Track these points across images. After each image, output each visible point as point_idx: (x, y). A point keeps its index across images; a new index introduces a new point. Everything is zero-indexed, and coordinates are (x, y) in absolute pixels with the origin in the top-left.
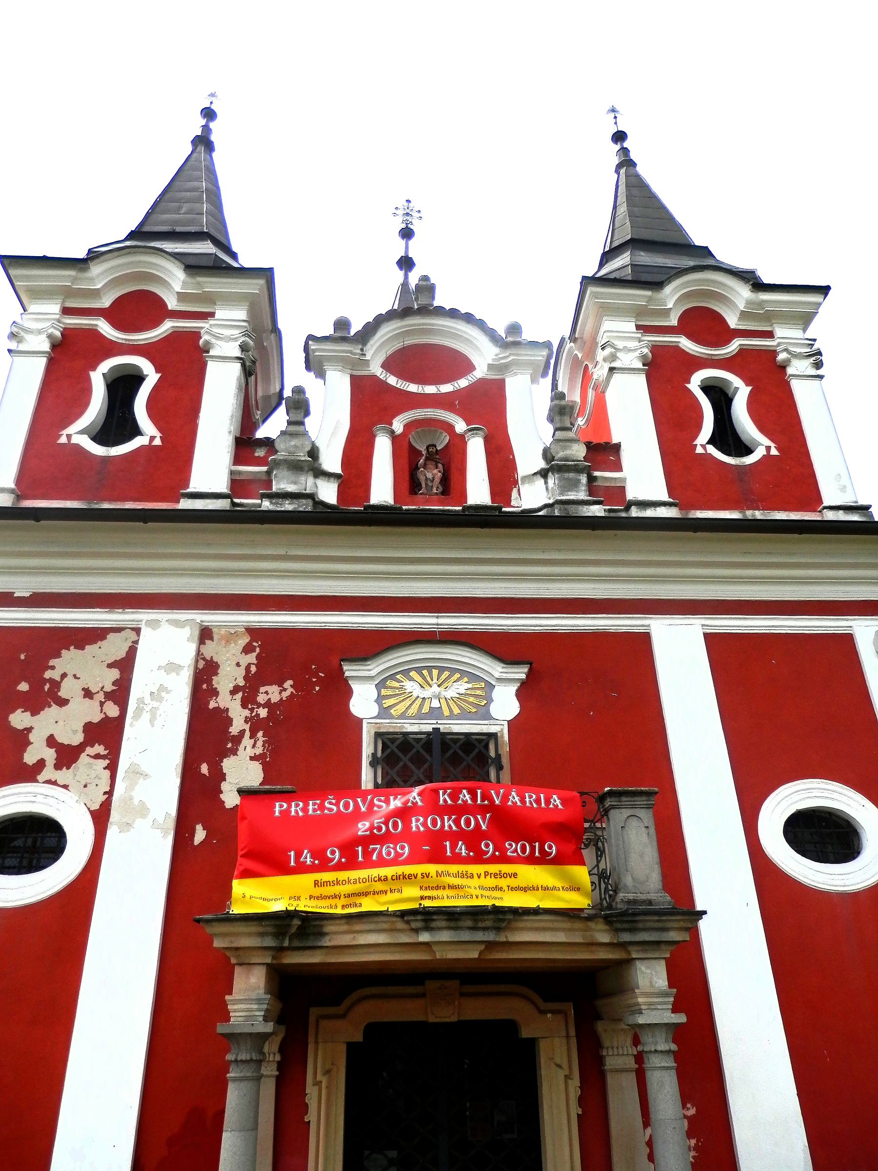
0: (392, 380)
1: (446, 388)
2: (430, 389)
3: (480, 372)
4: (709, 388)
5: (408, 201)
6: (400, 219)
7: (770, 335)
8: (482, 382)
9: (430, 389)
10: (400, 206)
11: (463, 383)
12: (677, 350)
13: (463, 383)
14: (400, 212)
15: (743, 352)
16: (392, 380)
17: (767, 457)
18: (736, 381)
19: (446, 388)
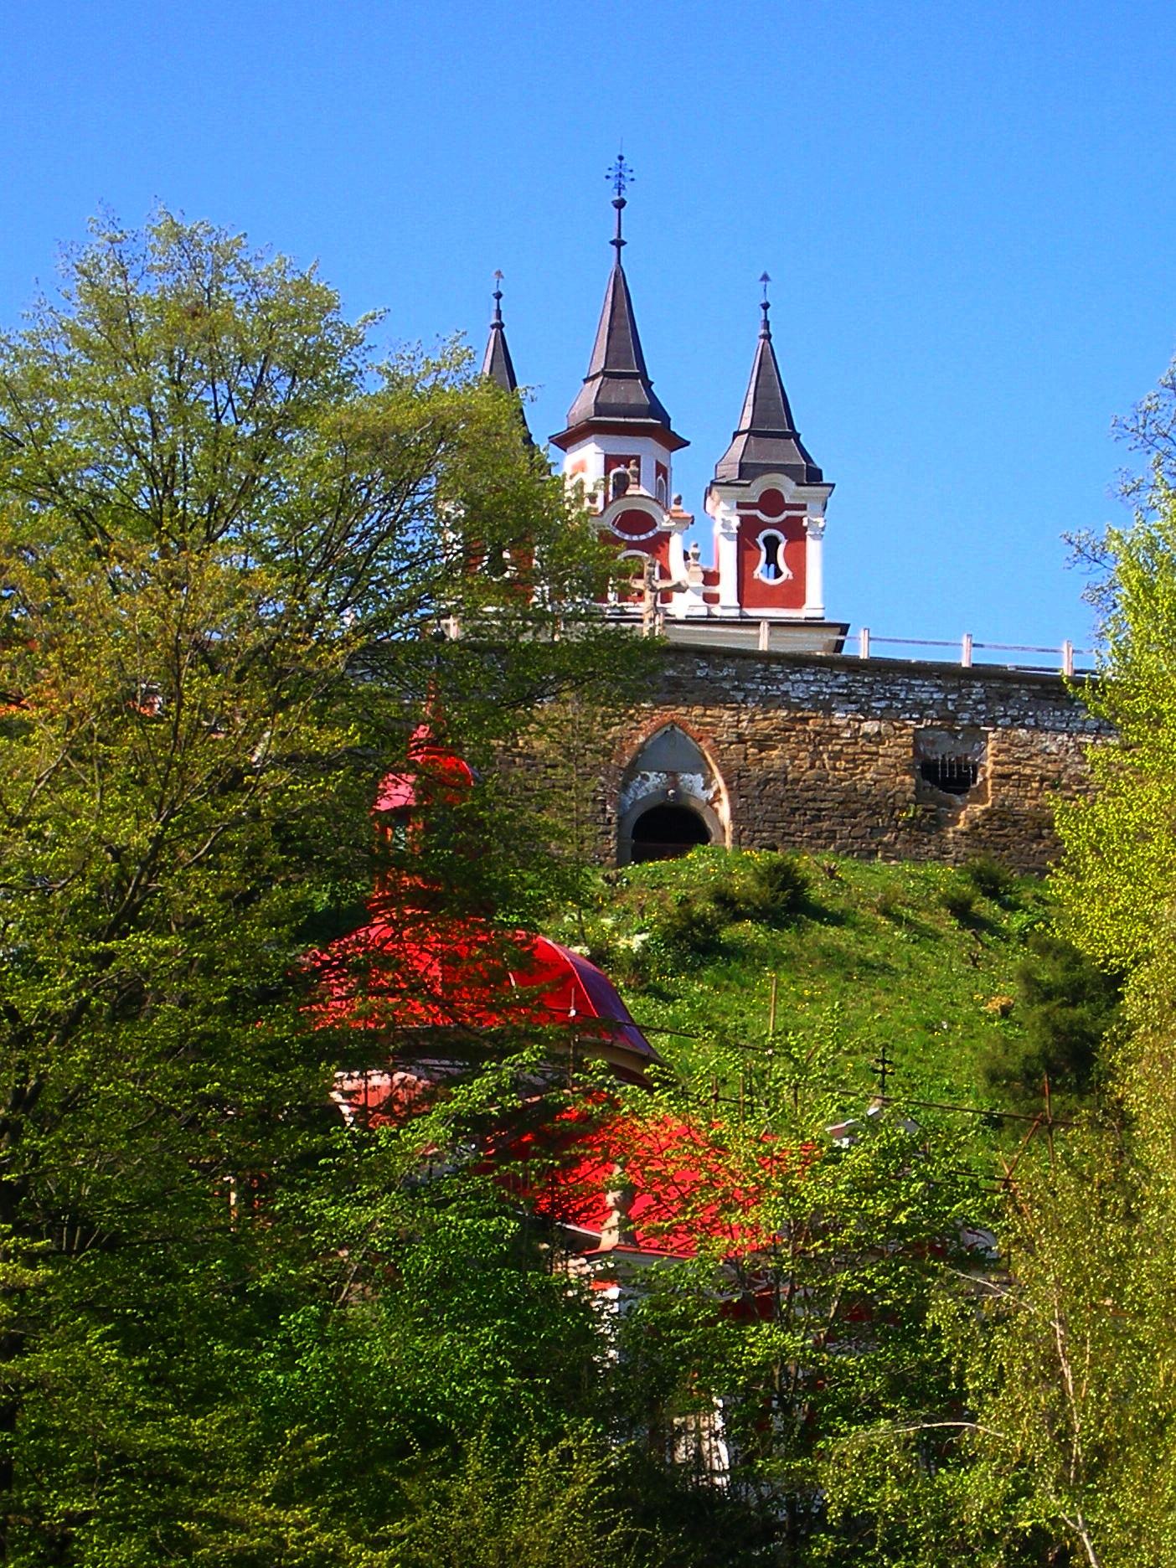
0: (617, 532)
1: (643, 537)
2: (635, 538)
3: (658, 529)
4: (765, 540)
5: (621, 158)
6: (612, 183)
7: (803, 507)
8: (660, 533)
9: (635, 538)
10: (612, 165)
11: (651, 534)
12: (756, 516)
13: (651, 534)
14: (612, 174)
15: (788, 517)
16: (617, 532)
17: (786, 581)
18: (781, 536)
19: (643, 537)
